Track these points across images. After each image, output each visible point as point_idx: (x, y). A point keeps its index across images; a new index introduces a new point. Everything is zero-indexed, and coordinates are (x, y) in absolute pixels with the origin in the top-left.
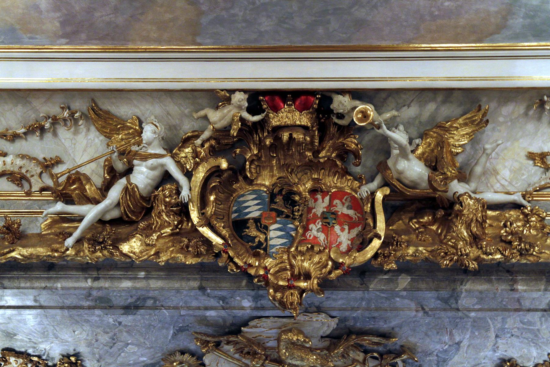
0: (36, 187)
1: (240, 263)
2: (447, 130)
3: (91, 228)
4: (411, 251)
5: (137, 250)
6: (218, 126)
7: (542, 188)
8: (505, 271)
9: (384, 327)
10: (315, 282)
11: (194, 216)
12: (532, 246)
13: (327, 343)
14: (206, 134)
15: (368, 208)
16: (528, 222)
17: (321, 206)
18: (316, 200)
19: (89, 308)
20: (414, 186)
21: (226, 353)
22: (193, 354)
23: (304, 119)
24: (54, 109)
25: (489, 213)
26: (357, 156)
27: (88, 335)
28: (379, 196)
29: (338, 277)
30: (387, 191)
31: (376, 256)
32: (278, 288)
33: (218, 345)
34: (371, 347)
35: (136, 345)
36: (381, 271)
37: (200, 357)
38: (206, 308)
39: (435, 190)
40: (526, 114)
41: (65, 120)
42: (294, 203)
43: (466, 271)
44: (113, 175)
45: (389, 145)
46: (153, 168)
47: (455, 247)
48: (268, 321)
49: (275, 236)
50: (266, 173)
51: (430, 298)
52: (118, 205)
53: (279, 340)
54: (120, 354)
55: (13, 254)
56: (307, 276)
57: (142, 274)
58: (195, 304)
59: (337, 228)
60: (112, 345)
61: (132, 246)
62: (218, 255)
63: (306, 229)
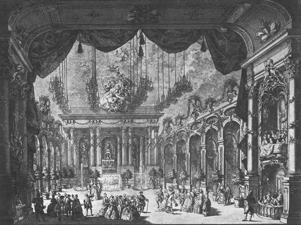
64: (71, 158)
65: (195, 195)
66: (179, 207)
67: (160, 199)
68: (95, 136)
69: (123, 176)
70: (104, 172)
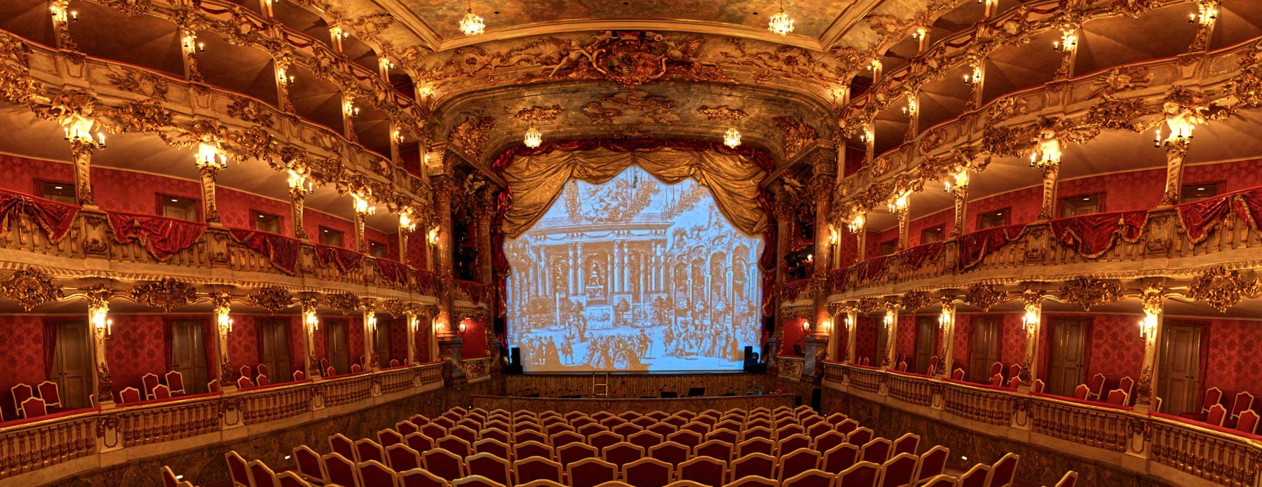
49: (625, 70)
51: (681, 88)
61: (573, 75)
64: (544, 290)
65: (718, 334)
66: (695, 350)
67: (669, 339)
68: (575, 255)
69: (616, 308)
70: (589, 303)
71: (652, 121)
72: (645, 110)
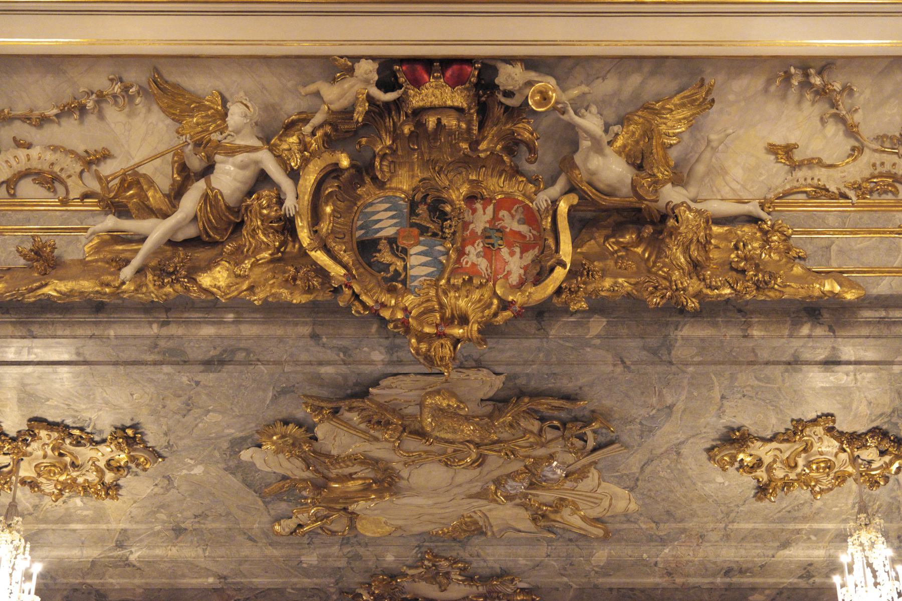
0: (75, 193)
1: (370, 303)
2: (657, 113)
3: (156, 252)
4: (607, 283)
5: (222, 284)
6: (335, 107)
7: (786, 194)
8: (735, 310)
9: (568, 385)
10: (475, 327)
11: (304, 235)
12: (773, 276)
13: (488, 408)
14: (318, 119)
15: (547, 223)
16: (767, 241)
17: (481, 219)
18: (474, 211)
19: (155, 363)
20: (610, 193)
21: (348, 424)
22: (300, 425)
23: (457, 98)
24: (100, 81)
25: (716, 229)
26: (532, 149)
27: (151, 400)
28: (563, 207)
29: (507, 322)
30: (574, 199)
31: (559, 291)
32: (422, 337)
33: (336, 411)
34: (550, 413)
35: (220, 412)
36: (565, 311)
37: (310, 429)
38: (321, 363)
39: (641, 198)
40: (766, 90)
41: (115, 96)
42: (444, 216)
43: (683, 311)
44: (186, 176)
45: (577, 133)
46: (243, 167)
47: (667, 278)
48: (407, 379)
49: (418, 263)
50: (403, 173)
51: (633, 348)
52: (195, 219)
53: (421, 405)
54: (196, 425)
55: (48, 290)
56: (464, 320)
57: (230, 317)
58: (304, 357)
59: (505, 251)
60: (185, 412)
61: (216, 278)
62: (337, 291)
63: (461, 253)
71: (521, 519)
72: (496, 465)
